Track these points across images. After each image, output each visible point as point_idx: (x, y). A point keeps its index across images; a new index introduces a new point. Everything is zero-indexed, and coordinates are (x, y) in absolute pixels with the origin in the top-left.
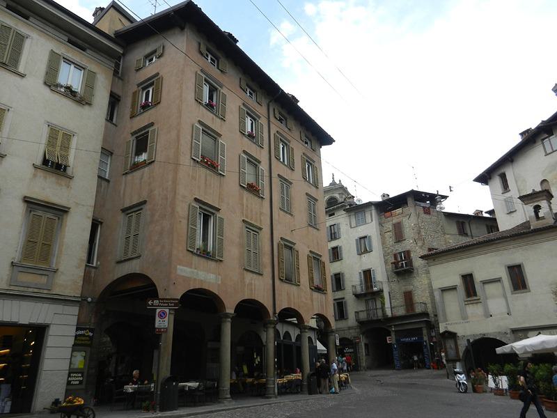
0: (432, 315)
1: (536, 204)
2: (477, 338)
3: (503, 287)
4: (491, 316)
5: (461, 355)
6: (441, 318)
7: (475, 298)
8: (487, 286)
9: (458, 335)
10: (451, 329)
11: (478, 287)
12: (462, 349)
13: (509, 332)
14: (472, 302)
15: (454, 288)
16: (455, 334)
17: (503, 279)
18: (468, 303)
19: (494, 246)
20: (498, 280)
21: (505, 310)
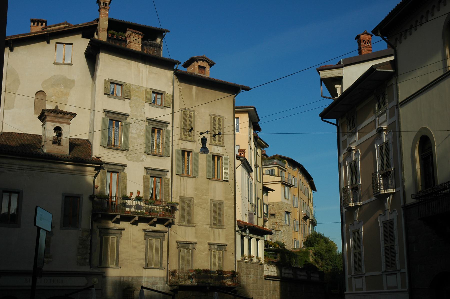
1: (58, 125)
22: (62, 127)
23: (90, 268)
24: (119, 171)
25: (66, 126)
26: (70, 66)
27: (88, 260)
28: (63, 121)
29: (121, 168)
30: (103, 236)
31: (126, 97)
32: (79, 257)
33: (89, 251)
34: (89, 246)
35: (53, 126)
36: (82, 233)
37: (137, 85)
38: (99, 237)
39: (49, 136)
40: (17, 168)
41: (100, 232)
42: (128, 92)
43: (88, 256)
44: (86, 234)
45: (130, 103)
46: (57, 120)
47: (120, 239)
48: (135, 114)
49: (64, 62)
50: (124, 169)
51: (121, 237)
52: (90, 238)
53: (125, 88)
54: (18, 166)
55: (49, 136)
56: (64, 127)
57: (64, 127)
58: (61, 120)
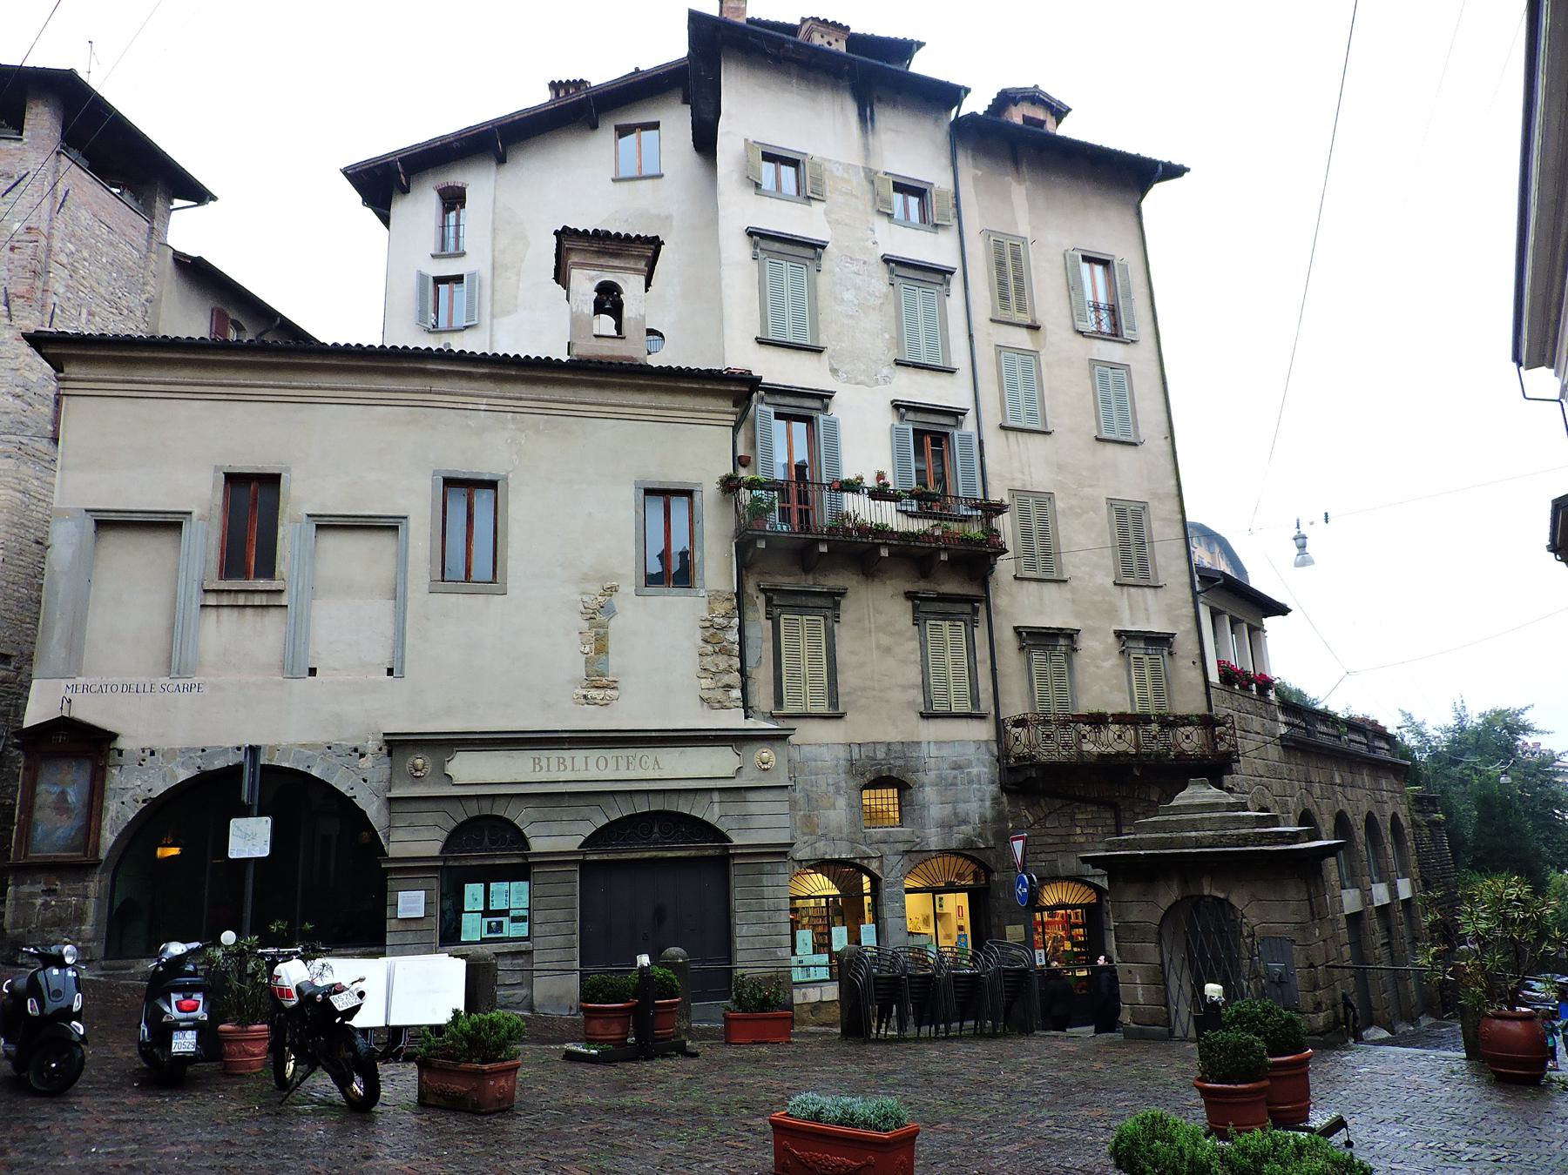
2: (218, 764)
3: (402, 559)
4: (313, 672)
5: (108, 838)
6: (52, 646)
7: (262, 584)
8: (331, 541)
9: (121, 743)
10: (88, 711)
11: (288, 536)
12: (119, 812)
13: (372, 745)
14: (241, 600)
15: (169, 524)
16: (113, 736)
17: (412, 523)
18: (215, 599)
19: (416, 383)
20: (389, 526)
21: (383, 657)
23: (746, 717)
24: (814, 414)
25: (632, 279)
26: (656, 181)
27: (736, 693)
28: (622, 265)
29: (816, 404)
30: (780, 615)
31: (812, 195)
32: (706, 683)
33: (736, 663)
34: (736, 647)
36: (710, 603)
37: (842, 161)
38: (767, 618)
40: (483, 407)
41: (769, 602)
42: (818, 182)
43: (735, 678)
44: (722, 608)
45: (826, 213)
46: (602, 261)
47: (836, 625)
48: (847, 244)
49: (640, 173)
50: (825, 408)
51: (838, 617)
52: (736, 620)
53: (808, 170)
54: (485, 401)
56: (626, 282)
57: (626, 282)
58: (616, 263)
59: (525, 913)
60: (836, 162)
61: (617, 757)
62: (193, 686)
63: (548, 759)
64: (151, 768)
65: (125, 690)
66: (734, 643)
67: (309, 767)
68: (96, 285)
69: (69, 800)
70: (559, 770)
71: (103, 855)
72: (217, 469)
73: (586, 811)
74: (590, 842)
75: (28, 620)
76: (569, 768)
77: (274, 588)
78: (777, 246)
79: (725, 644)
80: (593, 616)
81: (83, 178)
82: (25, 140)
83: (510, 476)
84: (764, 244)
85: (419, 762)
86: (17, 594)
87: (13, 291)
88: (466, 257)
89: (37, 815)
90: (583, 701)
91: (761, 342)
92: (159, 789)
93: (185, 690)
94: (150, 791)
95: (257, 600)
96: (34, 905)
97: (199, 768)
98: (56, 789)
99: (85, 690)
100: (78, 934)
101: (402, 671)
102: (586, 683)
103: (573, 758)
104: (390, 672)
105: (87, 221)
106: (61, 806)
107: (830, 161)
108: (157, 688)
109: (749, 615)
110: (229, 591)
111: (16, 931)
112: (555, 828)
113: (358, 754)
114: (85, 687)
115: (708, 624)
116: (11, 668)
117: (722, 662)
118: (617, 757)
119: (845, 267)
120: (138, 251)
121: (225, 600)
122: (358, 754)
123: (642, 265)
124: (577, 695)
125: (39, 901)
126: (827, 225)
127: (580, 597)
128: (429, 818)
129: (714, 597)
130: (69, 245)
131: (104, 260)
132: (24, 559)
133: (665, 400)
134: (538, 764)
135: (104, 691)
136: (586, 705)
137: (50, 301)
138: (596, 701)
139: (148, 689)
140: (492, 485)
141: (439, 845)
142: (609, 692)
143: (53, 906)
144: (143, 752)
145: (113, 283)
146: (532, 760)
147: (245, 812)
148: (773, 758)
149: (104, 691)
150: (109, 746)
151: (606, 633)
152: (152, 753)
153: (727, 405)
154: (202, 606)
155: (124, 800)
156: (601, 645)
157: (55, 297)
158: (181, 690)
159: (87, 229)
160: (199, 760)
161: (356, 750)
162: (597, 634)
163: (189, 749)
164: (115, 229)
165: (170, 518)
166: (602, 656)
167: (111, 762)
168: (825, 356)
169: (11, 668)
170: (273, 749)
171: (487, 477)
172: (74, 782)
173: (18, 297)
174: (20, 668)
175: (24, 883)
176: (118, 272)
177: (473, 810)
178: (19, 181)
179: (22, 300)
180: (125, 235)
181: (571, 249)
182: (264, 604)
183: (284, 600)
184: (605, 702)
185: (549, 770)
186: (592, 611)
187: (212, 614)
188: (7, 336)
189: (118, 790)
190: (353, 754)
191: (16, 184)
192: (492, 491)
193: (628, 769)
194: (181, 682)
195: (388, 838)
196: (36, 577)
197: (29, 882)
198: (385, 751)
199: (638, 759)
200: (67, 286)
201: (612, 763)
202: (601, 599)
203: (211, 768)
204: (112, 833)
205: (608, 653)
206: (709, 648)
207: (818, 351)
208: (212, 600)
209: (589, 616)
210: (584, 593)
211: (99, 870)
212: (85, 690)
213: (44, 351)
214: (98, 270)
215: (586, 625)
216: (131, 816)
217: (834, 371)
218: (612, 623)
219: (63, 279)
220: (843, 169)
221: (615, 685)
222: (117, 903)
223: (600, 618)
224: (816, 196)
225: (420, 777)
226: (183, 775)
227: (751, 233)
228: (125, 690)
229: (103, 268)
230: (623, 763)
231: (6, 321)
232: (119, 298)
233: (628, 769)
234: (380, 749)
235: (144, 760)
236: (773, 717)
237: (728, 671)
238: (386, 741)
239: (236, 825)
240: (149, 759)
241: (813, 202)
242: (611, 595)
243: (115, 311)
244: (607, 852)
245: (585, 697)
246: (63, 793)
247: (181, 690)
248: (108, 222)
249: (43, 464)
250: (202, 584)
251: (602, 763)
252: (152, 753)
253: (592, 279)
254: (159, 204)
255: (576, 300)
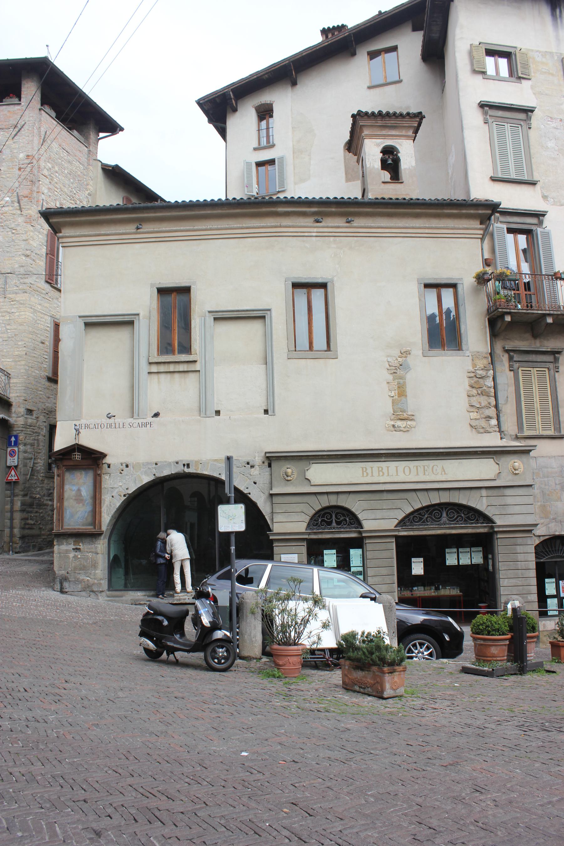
0: (22, 410)
1: (389, 142)
2: (166, 472)
3: (268, 338)
4: (218, 413)
7: (184, 357)
13: (258, 459)
14: (172, 368)
16: (103, 456)
22: (398, 146)
23: (501, 438)
24: (533, 228)
26: (398, 85)
27: (494, 422)
28: (397, 134)
29: (534, 221)
31: (522, 76)
32: (474, 415)
34: (492, 390)
35: (378, 145)
36: (473, 360)
39: (373, 165)
40: (314, 234)
41: (511, 359)
42: (526, 66)
43: (492, 412)
45: (532, 87)
46: (384, 132)
47: (557, 374)
49: (386, 81)
50: (541, 223)
51: (558, 368)
52: (491, 372)
54: (315, 230)
55: (373, 165)
56: (401, 145)
57: (401, 145)
58: (393, 132)
59: (361, 569)
60: (537, 51)
61: (417, 467)
62: (147, 423)
63: (372, 468)
64: (127, 475)
65: (108, 427)
66: (490, 387)
67: (220, 474)
68: (63, 187)
69: (82, 494)
70: (379, 475)
71: (104, 528)
72: (152, 285)
73: (398, 503)
74: (402, 523)
75: (40, 389)
76: (386, 474)
77: (191, 360)
78: (500, 113)
79: (484, 388)
80: (395, 371)
81: (53, 123)
82: (23, 104)
83: (335, 279)
84: (492, 112)
85: (289, 471)
86: (34, 374)
87: (21, 194)
88: (276, 147)
89: (66, 504)
90: (392, 428)
91: (494, 179)
92: (132, 488)
93: (143, 426)
94: (127, 489)
95: (182, 367)
96: (68, 557)
97: (154, 475)
98: (75, 488)
99: (86, 427)
100: (94, 575)
101: (274, 412)
102: (393, 417)
103: (388, 467)
104: (266, 412)
105: (57, 149)
106: (79, 499)
107: (532, 51)
108: (127, 425)
109: (498, 368)
110: (164, 363)
111: (60, 572)
112: (379, 514)
113: (249, 466)
114: (86, 425)
115: (472, 375)
116: (34, 417)
117: (484, 401)
118: (417, 467)
119: (548, 124)
120: (83, 165)
121: (162, 368)
122: (249, 466)
123: (410, 133)
124: (388, 425)
125: (72, 555)
126: (533, 96)
127: (386, 359)
128: (299, 507)
129: (475, 357)
130: (48, 164)
131: (66, 172)
132: (36, 352)
133: (434, 222)
134: (365, 471)
135: (97, 428)
136: (394, 432)
137: (41, 198)
138: (401, 429)
139: (121, 426)
140: (323, 286)
141: (305, 525)
142: (409, 423)
143: (79, 558)
144: (122, 465)
145: (71, 185)
146: (361, 469)
147: (227, 501)
148: (522, 466)
149: (97, 428)
150: (102, 461)
151: (405, 383)
152: (127, 466)
153: (476, 224)
154: (149, 373)
155: (113, 495)
156: (402, 391)
157: (43, 196)
158: (141, 426)
159: (56, 154)
160: (154, 470)
161: (248, 463)
162: (399, 383)
163: (148, 463)
164: (71, 153)
165: (127, 319)
166: (403, 398)
167: (104, 471)
168: (538, 186)
169: (34, 417)
170: (197, 462)
171: (320, 281)
172: (84, 483)
173: (25, 197)
174: (37, 418)
175: (63, 544)
176: (74, 179)
177: (325, 502)
178: (21, 129)
179: (26, 199)
180: (76, 156)
181: (363, 125)
182: (186, 370)
183: (197, 367)
184: (407, 429)
185: (372, 476)
186: (394, 368)
187: (155, 377)
188: (20, 221)
189: (109, 489)
190: (247, 466)
191: (19, 131)
192: (322, 291)
193: (424, 474)
194: (140, 421)
195: (272, 520)
196: (42, 363)
197: (65, 544)
198: (266, 464)
199: (431, 468)
200: (49, 189)
201: (414, 470)
202: (400, 359)
203: (162, 475)
204: (108, 515)
205: (406, 396)
206: (474, 392)
207: (533, 184)
208: (154, 369)
209: (392, 371)
210: (388, 356)
211: (102, 537)
212: (86, 427)
213: (51, 221)
214: (63, 178)
215: (391, 378)
216: (118, 505)
217: (545, 197)
218: (408, 376)
219: (47, 185)
220: (542, 55)
221: (413, 417)
222: (111, 558)
223: (400, 372)
224: (524, 76)
225: (290, 480)
226: (146, 479)
227: (483, 106)
228: (108, 427)
229: (66, 177)
230: (421, 470)
231: (19, 212)
232: (75, 194)
233: (424, 474)
234: (263, 463)
235: (122, 470)
236: (517, 438)
237: (488, 407)
238: (268, 457)
239: (222, 510)
240: (125, 469)
241: (523, 81)
242: (406, 357)
243: (73, 202)
244: (413, 530)
245: (394, 426)
246: (79, 490)
247: (141, 426)
248: (67, 149)
249: (42, 295)
250: (148, 359)
251: (407, 471)
252: (127, 466)
253: (378, 145)
254: (92, 136)
255: (369, 159)
